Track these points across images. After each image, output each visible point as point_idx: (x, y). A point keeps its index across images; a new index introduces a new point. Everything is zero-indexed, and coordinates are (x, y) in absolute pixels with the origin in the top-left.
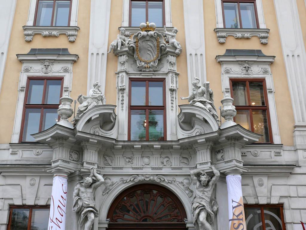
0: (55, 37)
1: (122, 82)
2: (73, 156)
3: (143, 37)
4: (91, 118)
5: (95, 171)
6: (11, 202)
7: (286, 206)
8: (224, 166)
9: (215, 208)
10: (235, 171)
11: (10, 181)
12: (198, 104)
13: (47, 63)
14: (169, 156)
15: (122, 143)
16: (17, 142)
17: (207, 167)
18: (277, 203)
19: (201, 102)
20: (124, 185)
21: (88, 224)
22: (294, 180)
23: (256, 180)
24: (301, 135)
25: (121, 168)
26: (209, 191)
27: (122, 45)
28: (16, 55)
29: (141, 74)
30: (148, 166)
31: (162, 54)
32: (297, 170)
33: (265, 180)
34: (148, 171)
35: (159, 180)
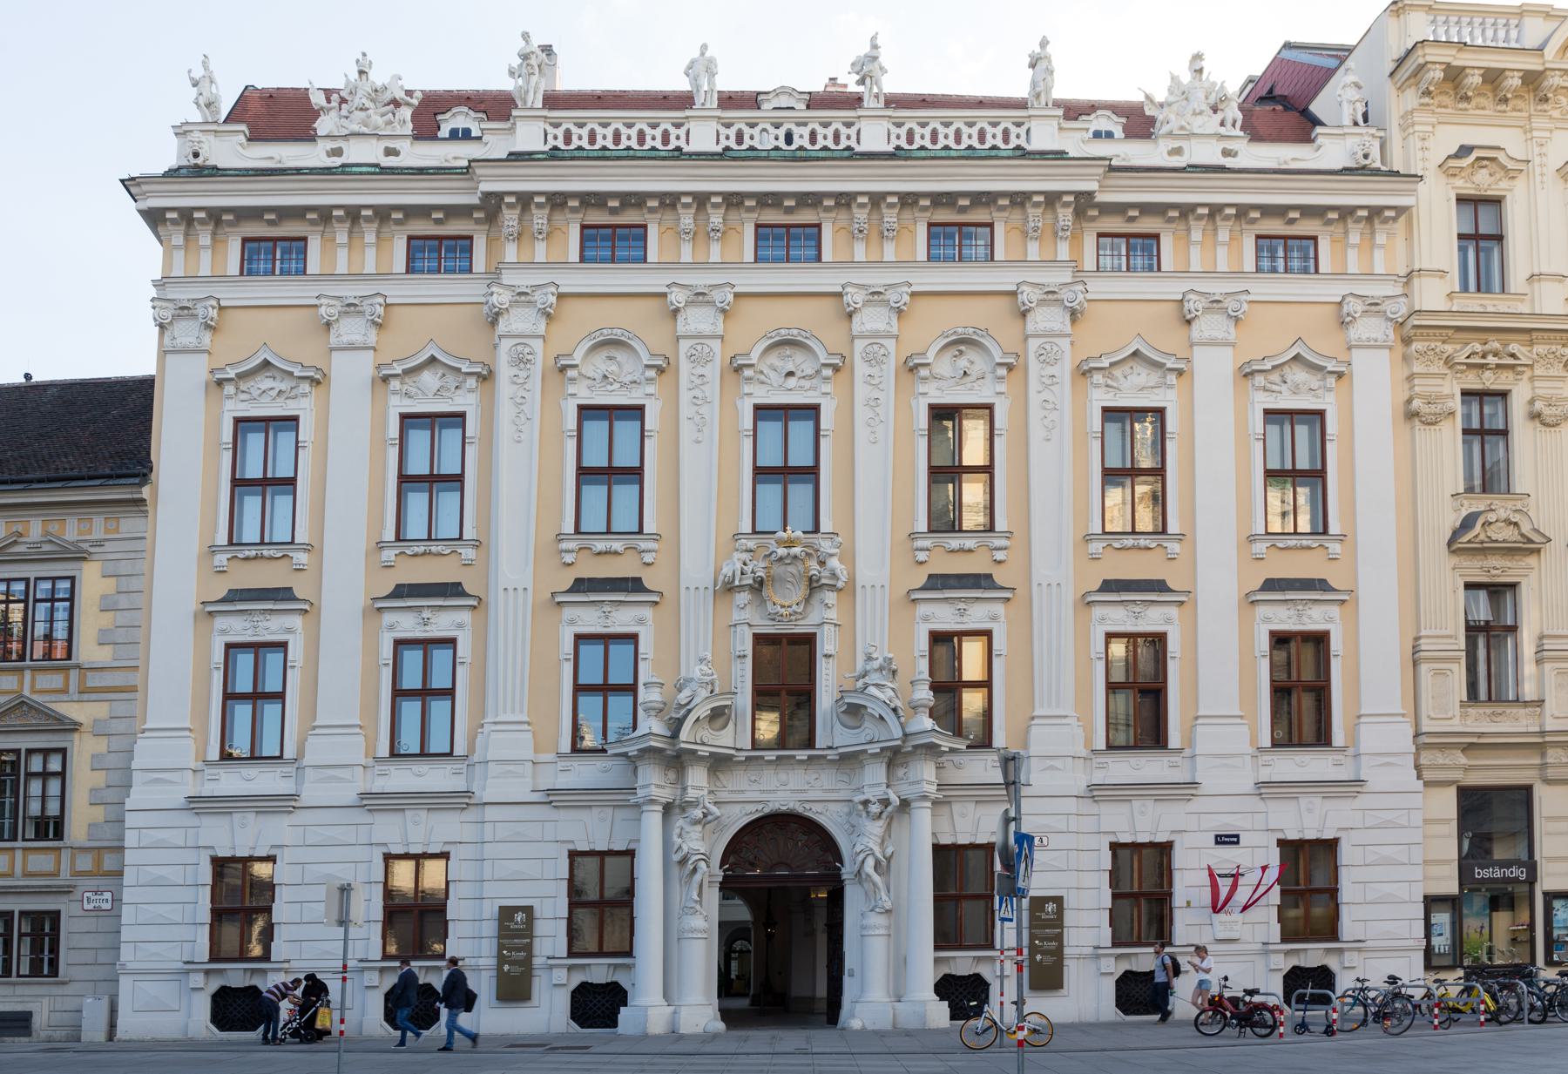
0: (616, 553)
1: (743, 643)
3: (781, 559)
6: (571, 847)
8: (907, 791)
9: (889, 851)
10: (925, 798)
12: (873, 690)
16: (568, 750)
17: (880, 792)
19: (877, 685)
21: (698, 877)
28: (122, 181)
31: (814, 586)
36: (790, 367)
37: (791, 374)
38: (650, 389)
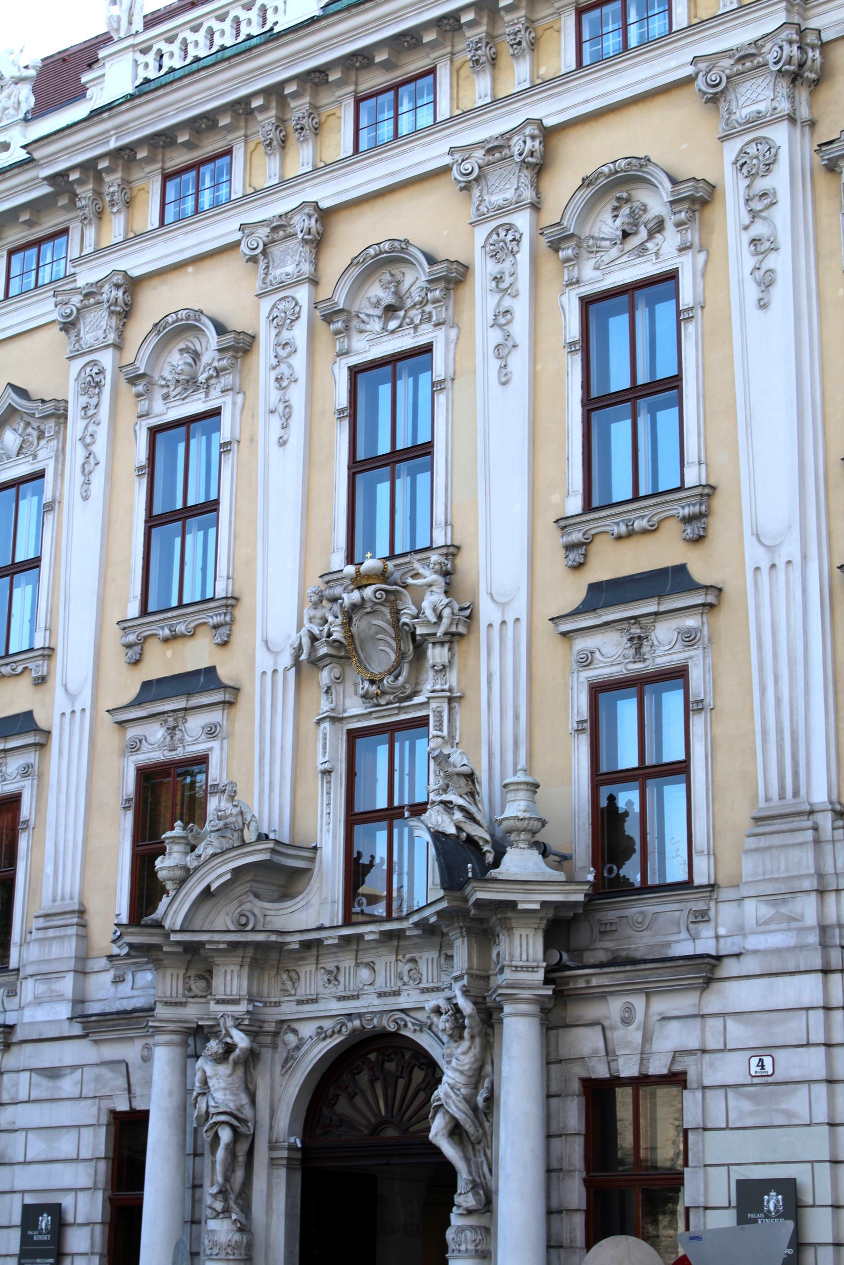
0: (183, 636)
2: (193, 987)
4: (209, 887)
5: (230, 1022)
7: (691, 1077)
11: (111, 1052)
14: (416, 955)
18: (665, 1071)
20: (322, 1044)
23: (615, 1007)
24: (757, 850)
25: (315, 1001)
26: (464, 1053)
27: (314, 639)
29: (371, 713)
30: (370, 989)
32: (730, 968)
34: (369, 1003)
35: (392, 1025)
36: (387, 298)
37: (390, 310)
38: (227, 380)
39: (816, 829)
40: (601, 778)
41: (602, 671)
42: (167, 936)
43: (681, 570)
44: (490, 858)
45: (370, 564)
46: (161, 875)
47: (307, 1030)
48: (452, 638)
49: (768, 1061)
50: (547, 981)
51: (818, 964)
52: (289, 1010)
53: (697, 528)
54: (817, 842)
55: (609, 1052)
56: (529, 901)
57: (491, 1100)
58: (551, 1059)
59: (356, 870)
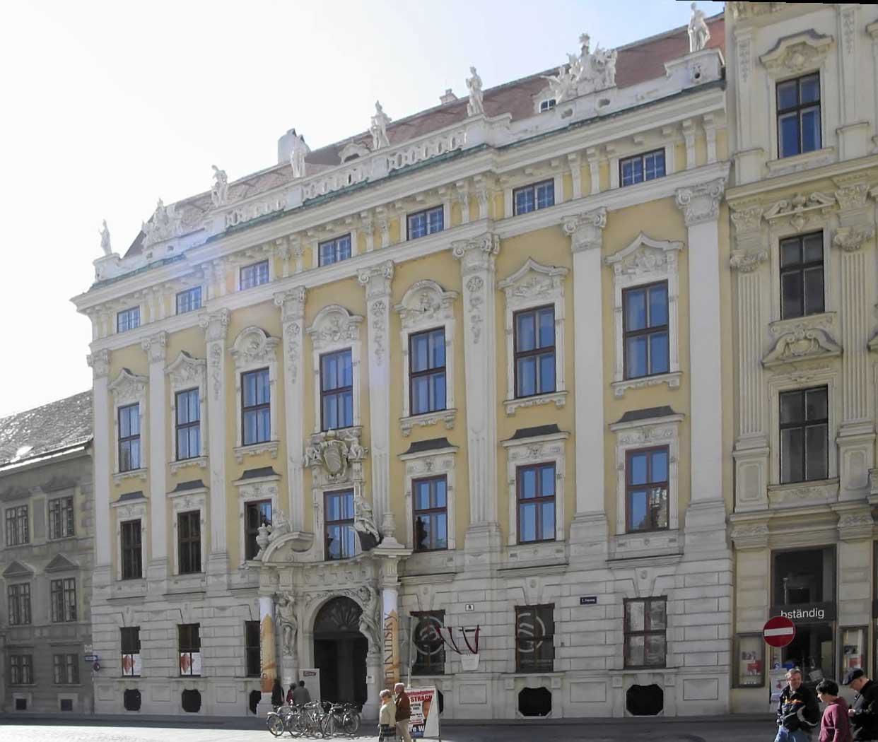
13: (256, 485)
15: (309, 565)
22: (456, 586)
23: (422, 588)
27: (310, 459)
33: (430, 587)
34: (335, 587)
39: (489, 531)
40: (416, 512)
41: (417, 475)
42: (263, 564)
43: (445, 439)
44: (378, 540)
45: (331, 433)
46: (258, 542)
47: (314, 595)
48: (361, 461)
49: (472, 606)
50: (399, 581)
51: (488, 574)
52: (307, 588)
53: (450, 423)
54: (490, 536)
55: (419, 603)
56: (393, 555)
57: (379, 619)
58: (400, 605)
59: (328, 541)
